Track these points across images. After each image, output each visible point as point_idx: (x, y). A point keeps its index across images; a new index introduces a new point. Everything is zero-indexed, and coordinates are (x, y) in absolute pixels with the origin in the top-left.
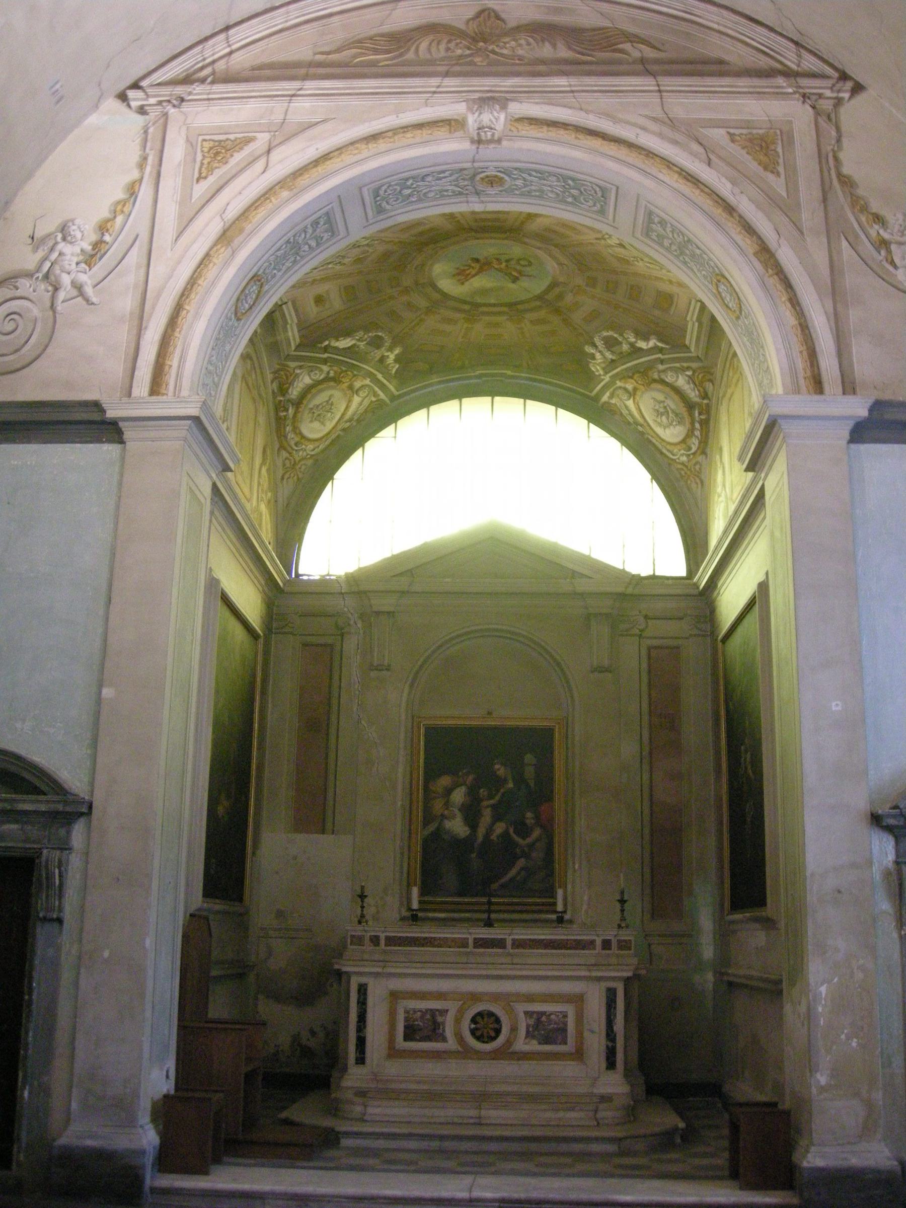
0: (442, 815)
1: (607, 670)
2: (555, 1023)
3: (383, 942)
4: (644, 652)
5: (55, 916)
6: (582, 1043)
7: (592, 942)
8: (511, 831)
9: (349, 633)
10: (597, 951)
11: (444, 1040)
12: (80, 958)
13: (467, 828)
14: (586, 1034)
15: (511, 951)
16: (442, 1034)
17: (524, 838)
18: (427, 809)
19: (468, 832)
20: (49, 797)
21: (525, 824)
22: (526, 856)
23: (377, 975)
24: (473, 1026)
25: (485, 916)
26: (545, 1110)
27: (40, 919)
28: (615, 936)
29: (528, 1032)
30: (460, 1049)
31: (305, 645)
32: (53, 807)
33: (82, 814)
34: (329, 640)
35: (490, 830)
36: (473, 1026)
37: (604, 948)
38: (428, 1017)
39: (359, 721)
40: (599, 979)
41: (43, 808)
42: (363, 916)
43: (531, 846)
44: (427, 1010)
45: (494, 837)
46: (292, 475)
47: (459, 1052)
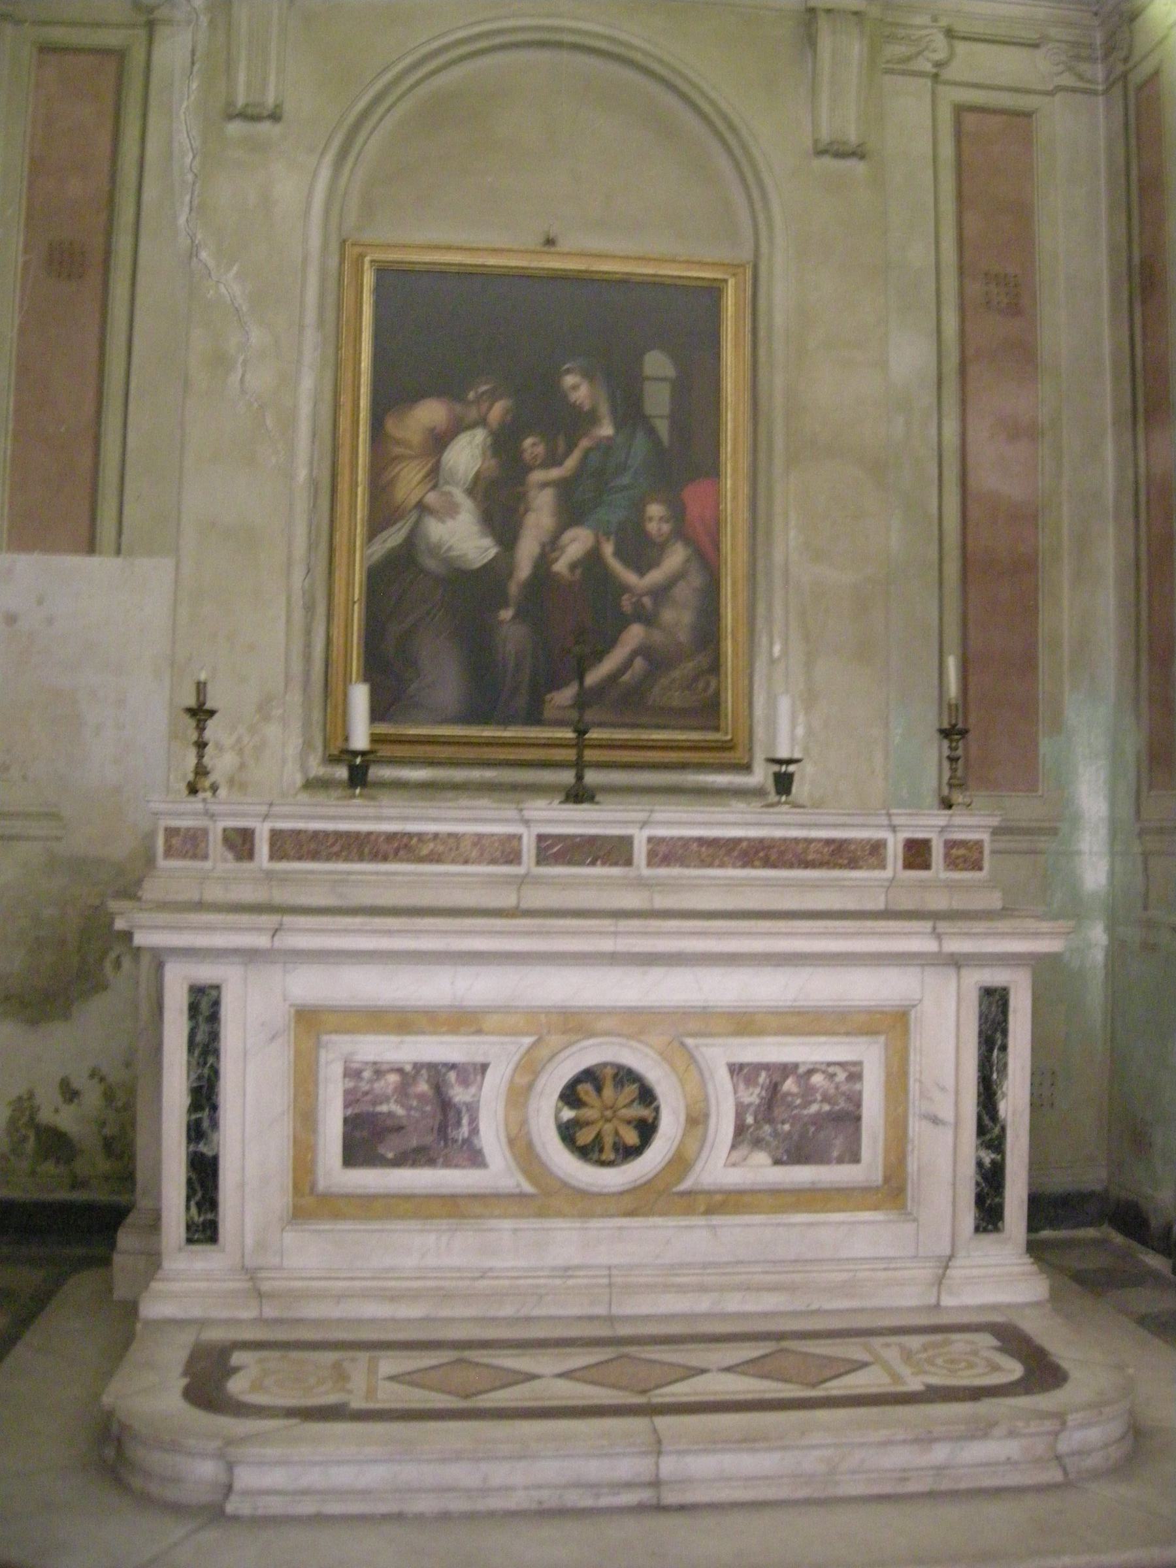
0: (422, 508)
1: (858, 154)
2: (826, 1099)
3: (263, 848)
4: (946, 116)
6: (902, 1160)
7: (876, 849)
8: (608, 549)
9: (169, 22)
10: (888, 873)
11: (476, 1159)
13: (487, 542)
14: (916, 1126)
15: (646, 872)
16: (467, 1142)
17: (641, 571)
18: (380, 488)
19: (493, 552)
21: (646, 535)
22: (648, 619)
23: (250, 956)
24: (568, 1114)
25: (567, 777)
26: (887, 1443)
28: (943, 829)
29: (740, 1130)
30: (528, 1188)
31: (46, 49)
35: (551, 547)
36: (568, 1114)
37: (909, 865)
38: (423, 1087)
39: (193, 252)
40: (957, 962)
42: (201, 771)
43: (661, 593)
44: (418, 1067)
45: (561, 566)
47: (522, 1196)
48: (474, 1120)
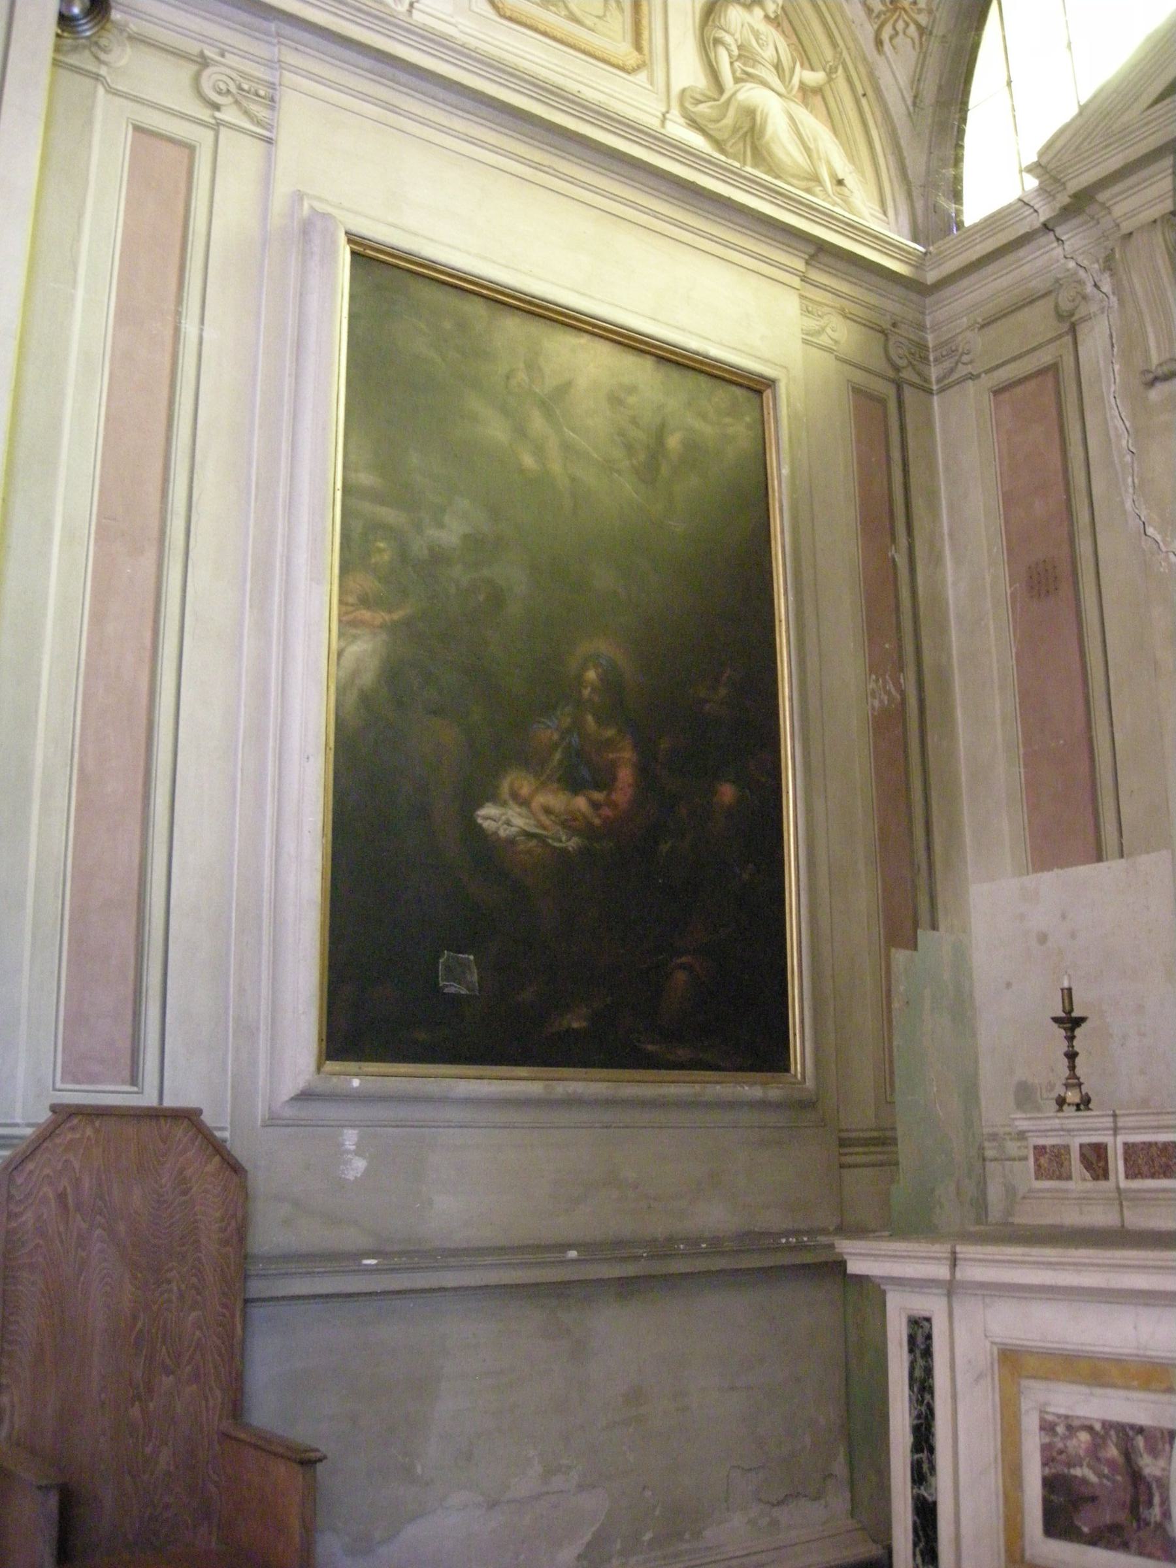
3: (1117, 1165)
9: (1085, 319)
16: (1160, 1526)
31: (997, 392)
34: (1045, 357)
38: (1112, 1452)
44: (1108, 1425)
46: (900, 25)
48: (1165, 1501)
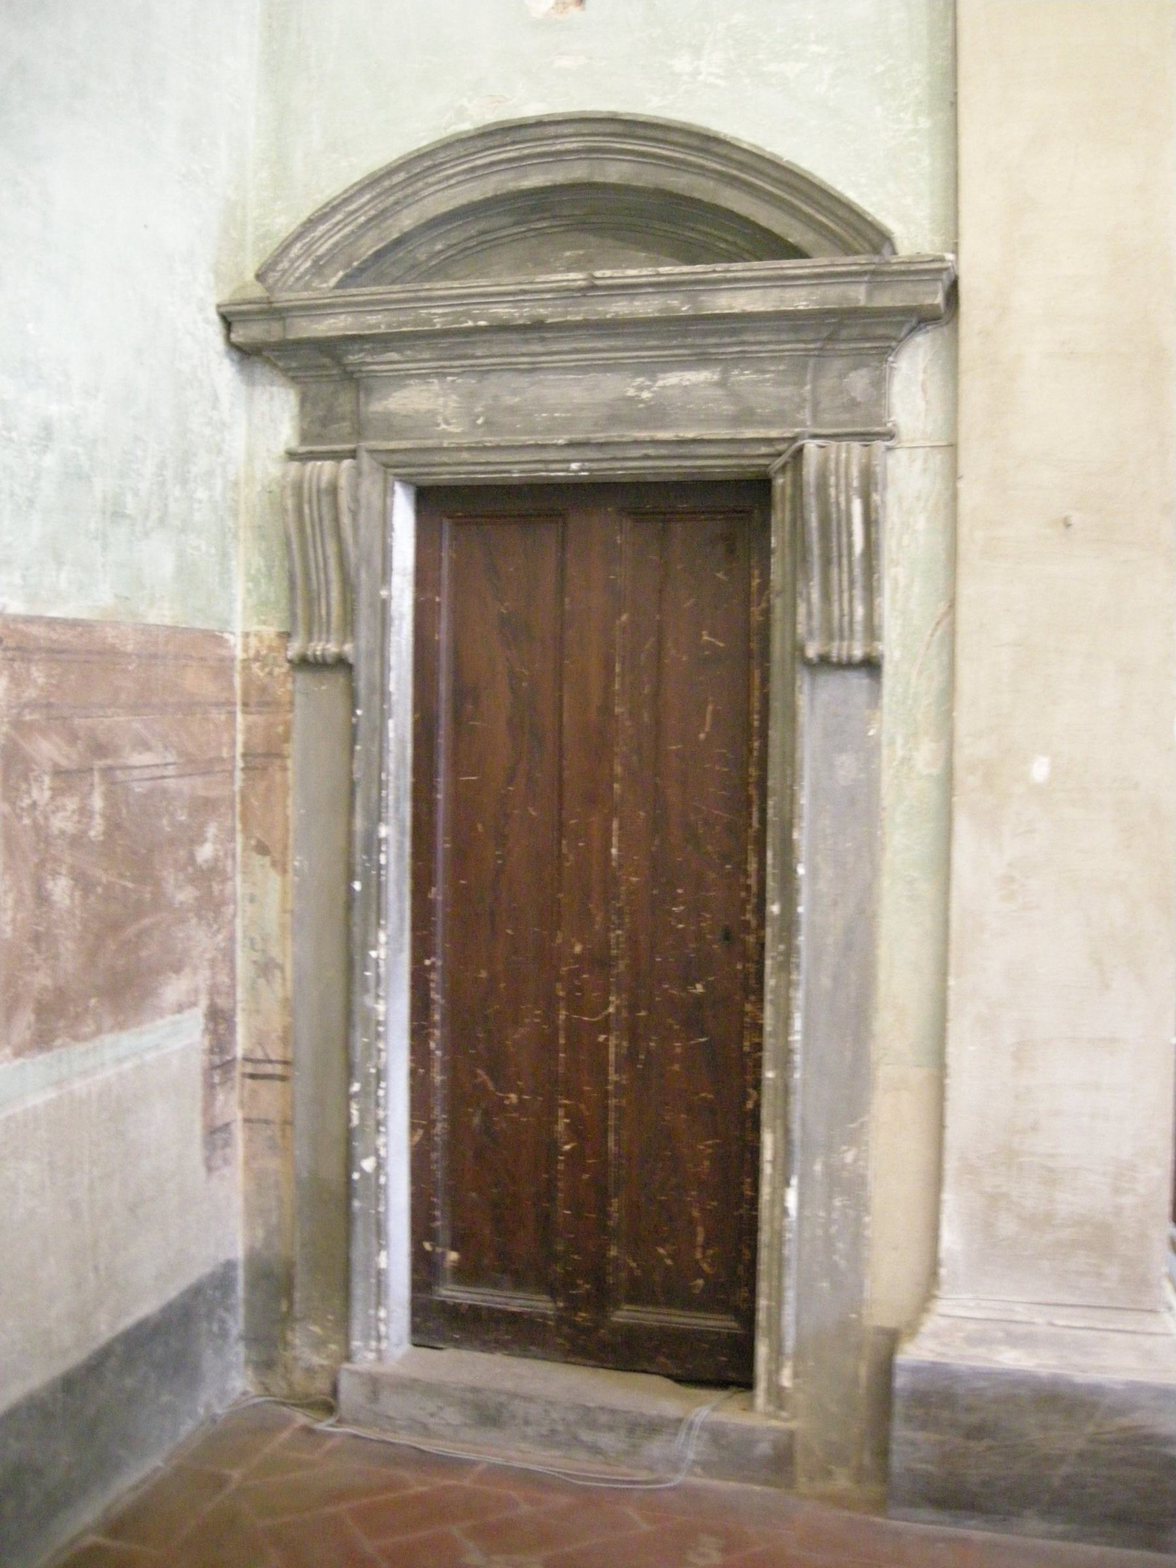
5: (858, 653)
12: (948, 780)
20: (819, 263)
27: (808, 664)
32: (831, 296)
33: (924, 319)
41: (800, 300)
